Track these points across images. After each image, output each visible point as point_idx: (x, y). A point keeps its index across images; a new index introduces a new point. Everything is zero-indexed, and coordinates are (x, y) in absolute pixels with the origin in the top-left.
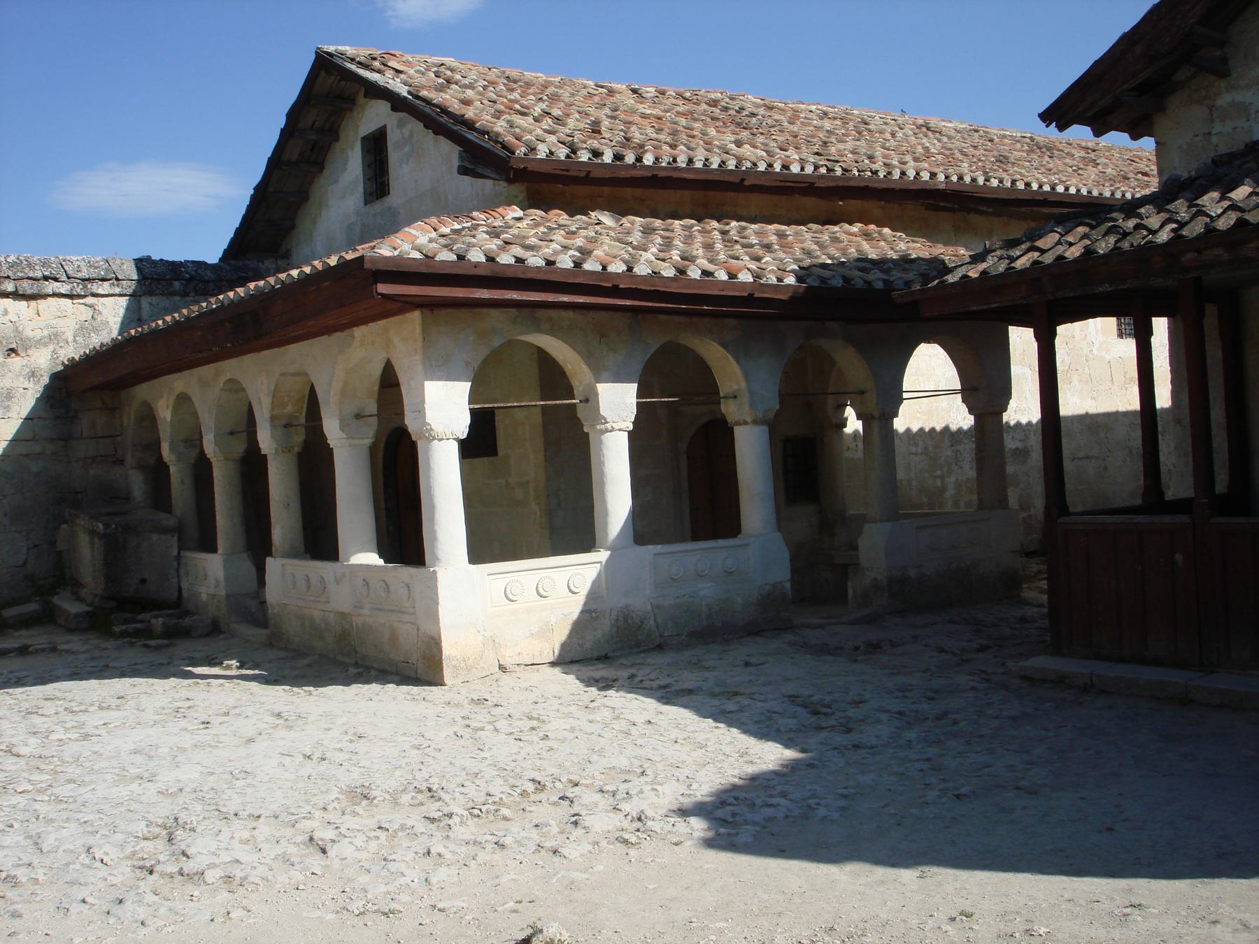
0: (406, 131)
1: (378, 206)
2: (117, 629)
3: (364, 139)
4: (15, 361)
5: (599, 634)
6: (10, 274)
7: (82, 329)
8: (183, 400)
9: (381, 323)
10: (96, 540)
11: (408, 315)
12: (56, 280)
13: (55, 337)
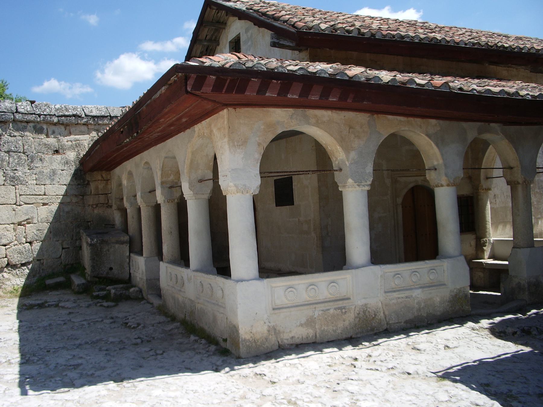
2: (95, 294)
3: (230, 42)
4: (58, 157)
5: (347, 323)
8: (130, 174)
9: (208, 120)
11: (221, 113)
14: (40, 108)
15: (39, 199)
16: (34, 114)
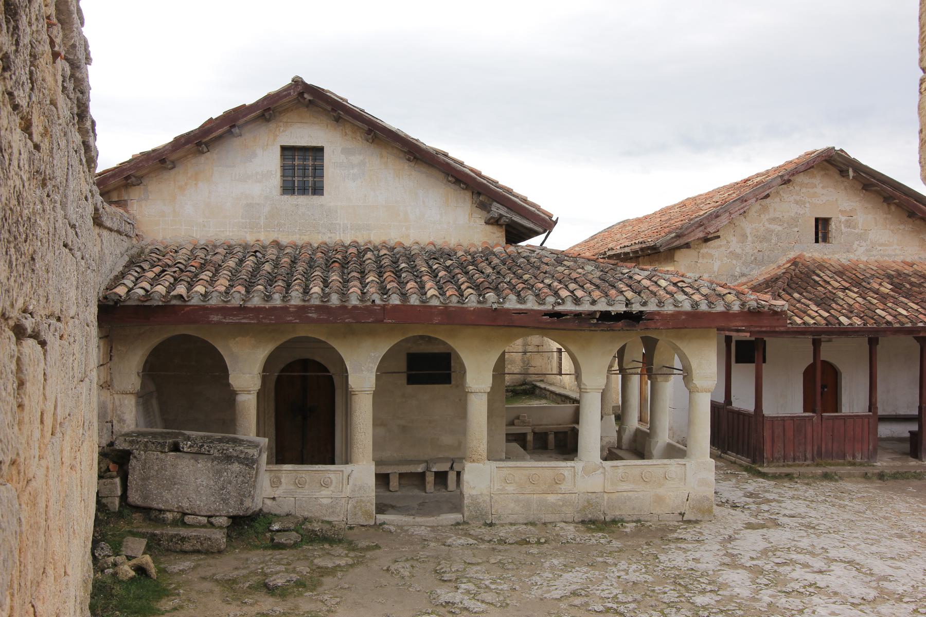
0: (356, 159)
1: (302, 200)
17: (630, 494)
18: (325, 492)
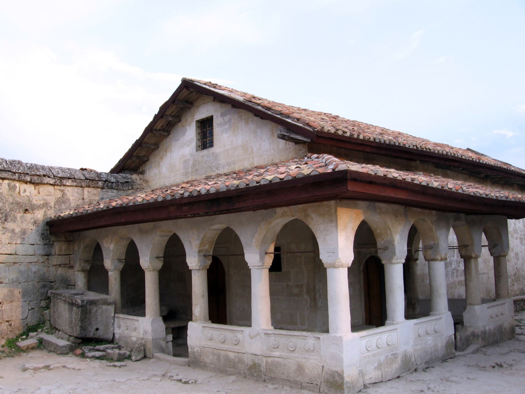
0: (227, 118)
1: (205, 152)
3: (197, 121)
4: (28, 216)
6: (29, 172)
7: (62, 201)
10: (75, 308)
12: (49, 177)
13: (46, 205)
14: (15, 166)
15: (11, 259)
16: (10, 171)
17: (280, 360)
18: (134, 334)
